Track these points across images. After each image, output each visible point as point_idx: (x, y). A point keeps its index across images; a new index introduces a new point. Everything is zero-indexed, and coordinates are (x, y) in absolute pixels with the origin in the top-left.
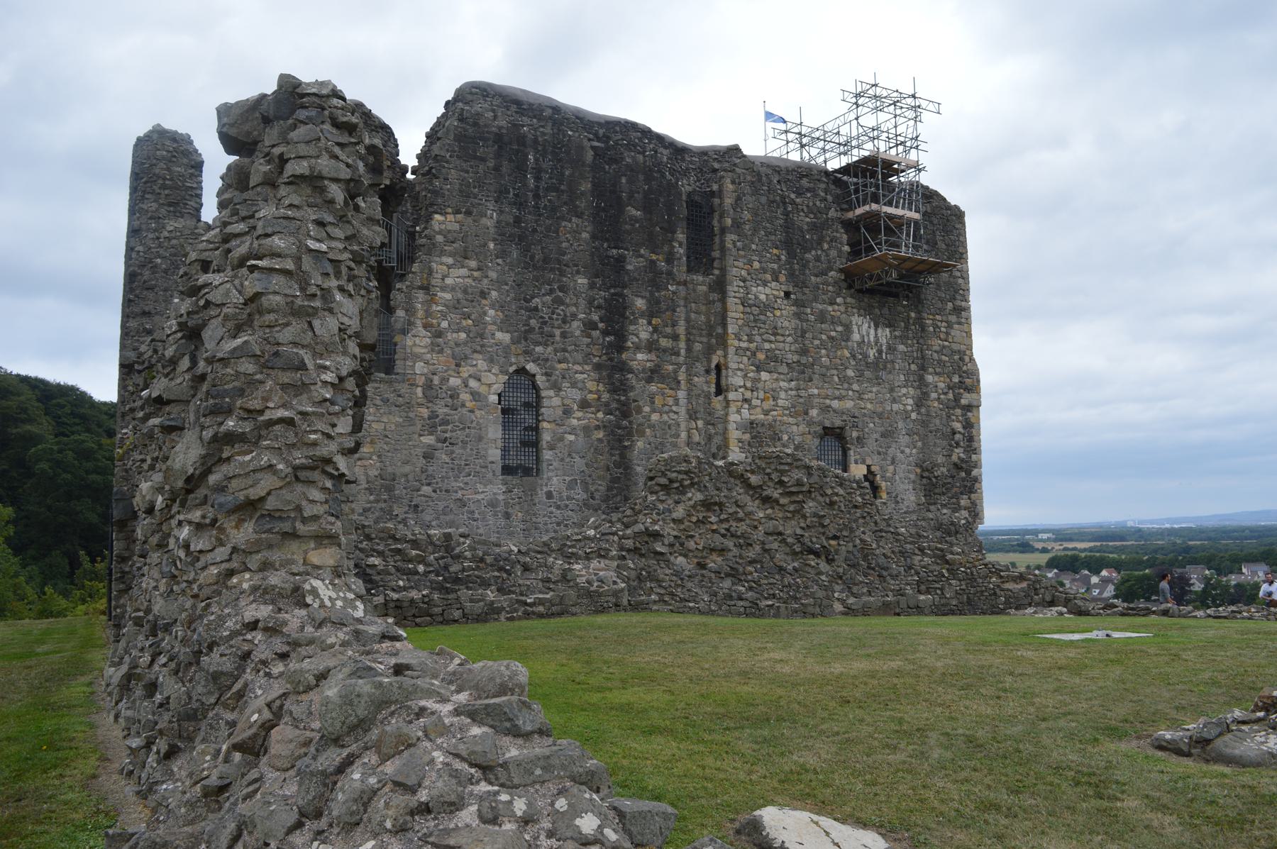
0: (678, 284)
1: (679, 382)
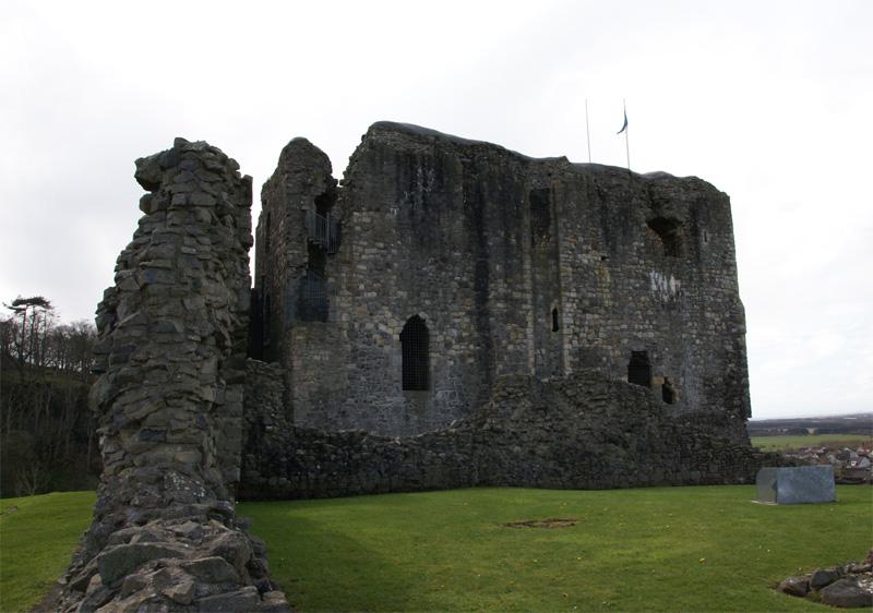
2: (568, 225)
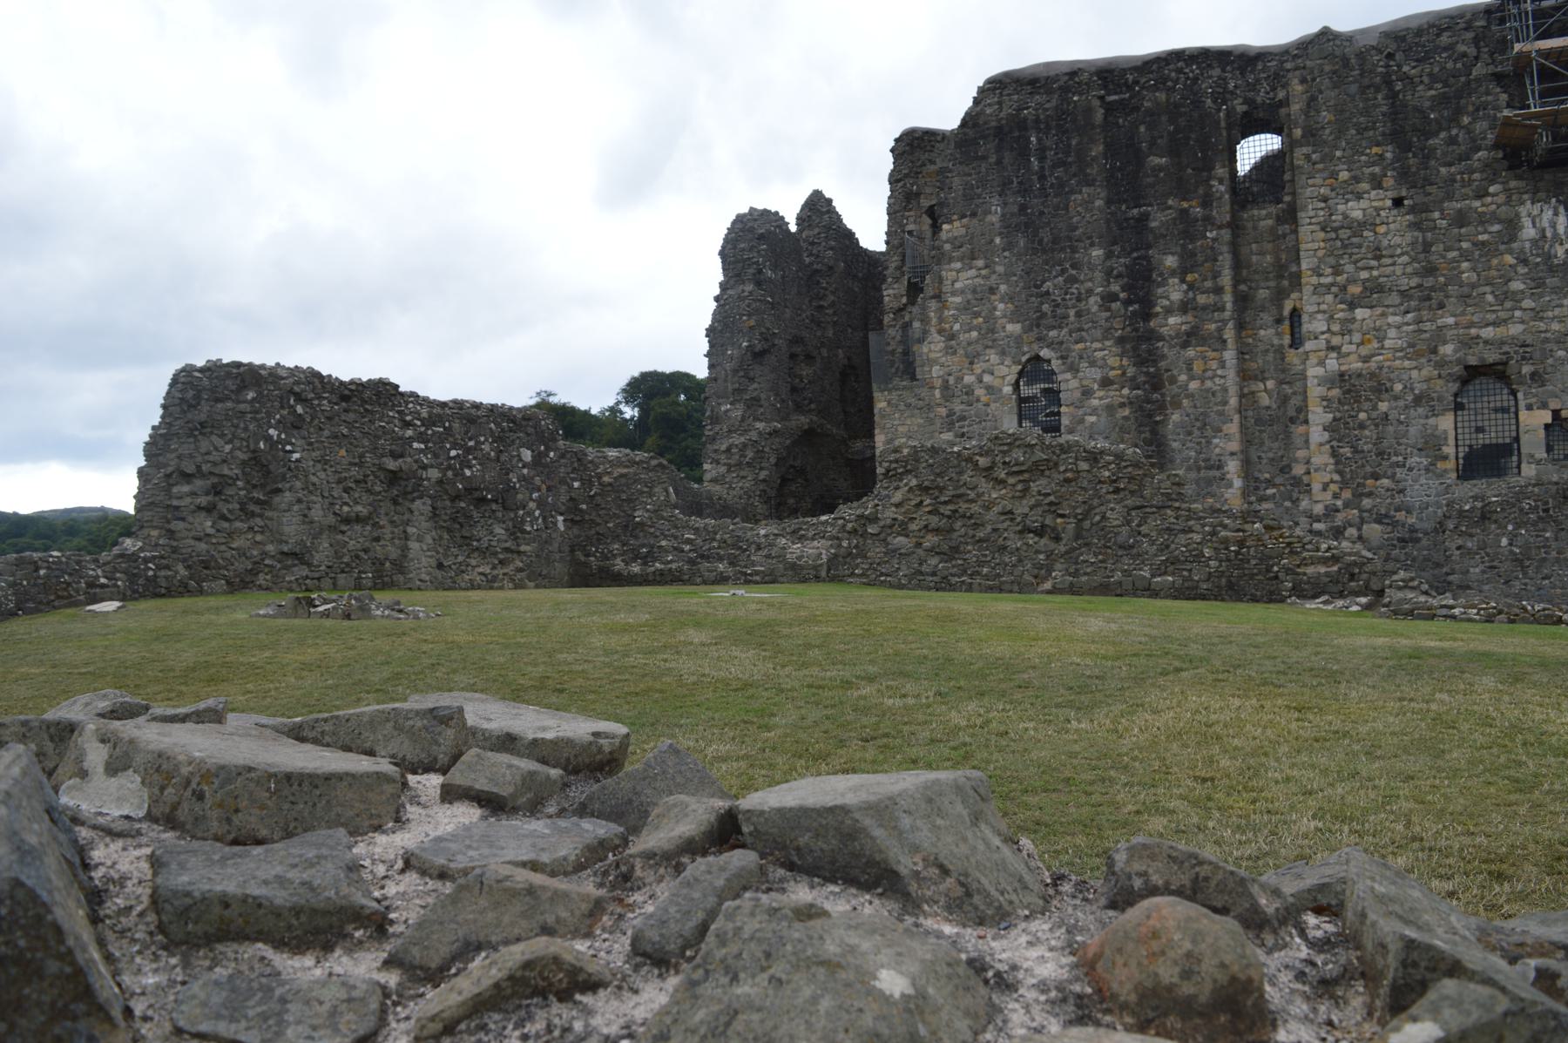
0: (1220, 227)
1: (1225, 341)
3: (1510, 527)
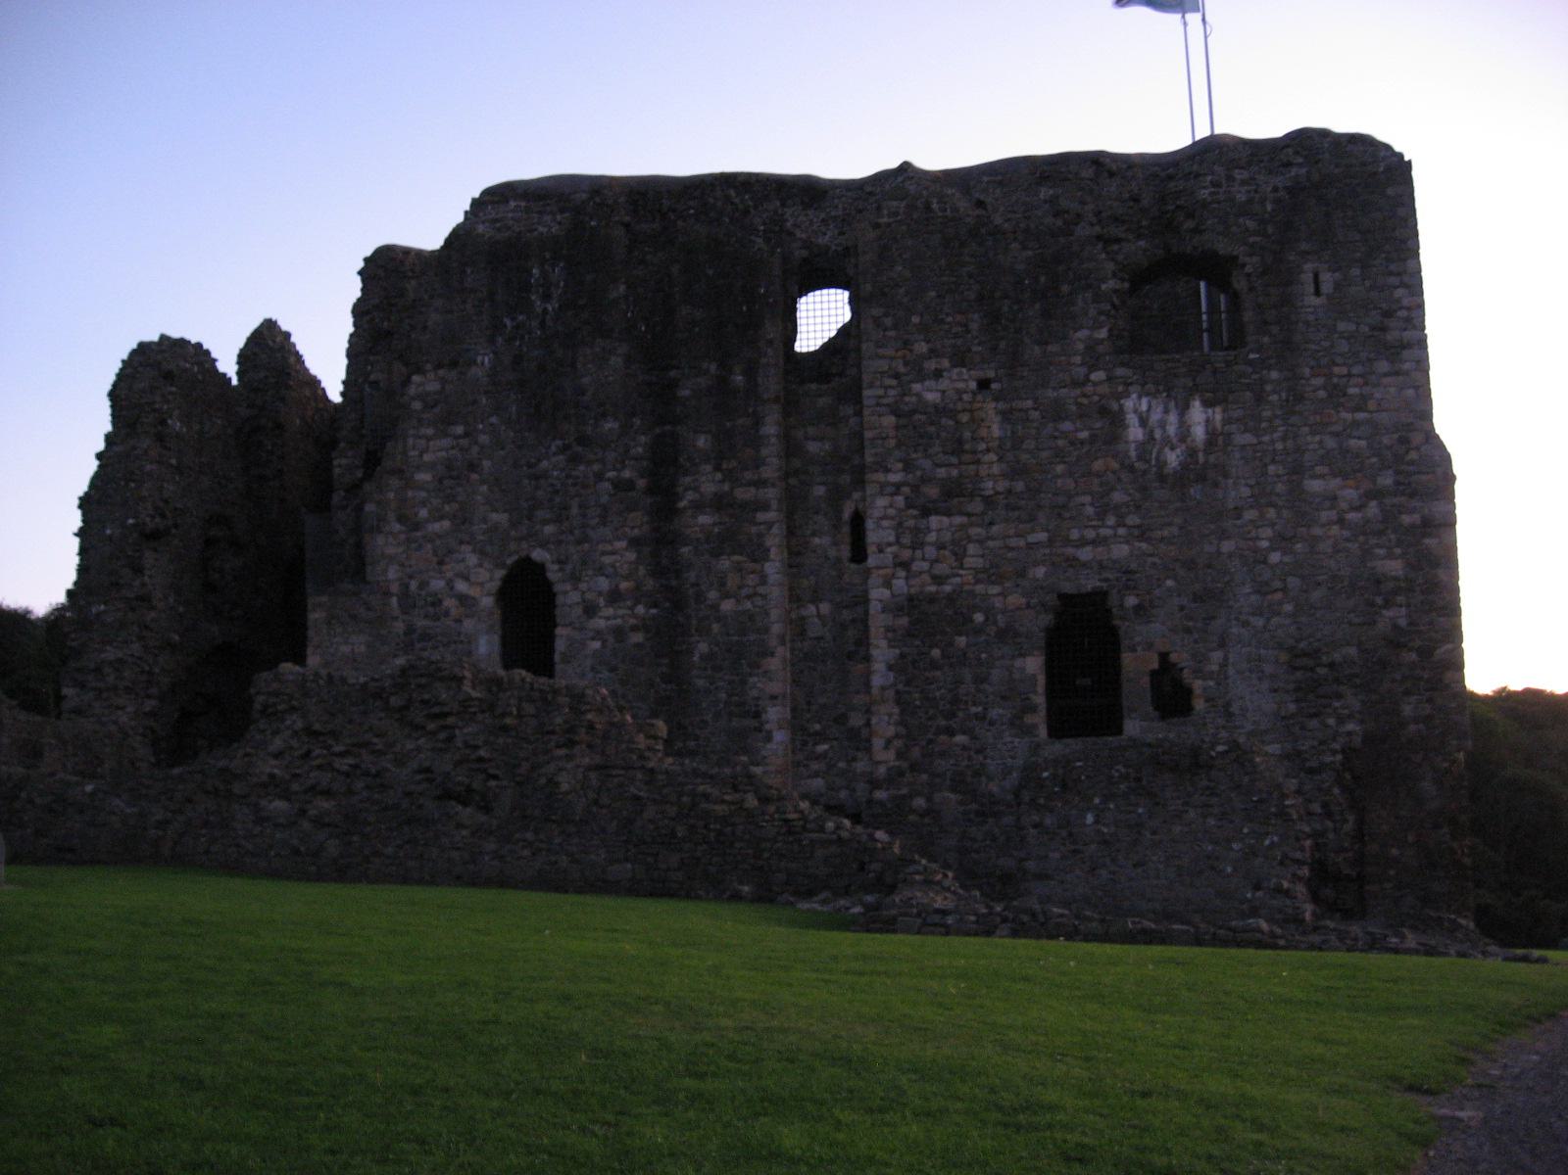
2: (888, 321)
3: (1097, 801)
